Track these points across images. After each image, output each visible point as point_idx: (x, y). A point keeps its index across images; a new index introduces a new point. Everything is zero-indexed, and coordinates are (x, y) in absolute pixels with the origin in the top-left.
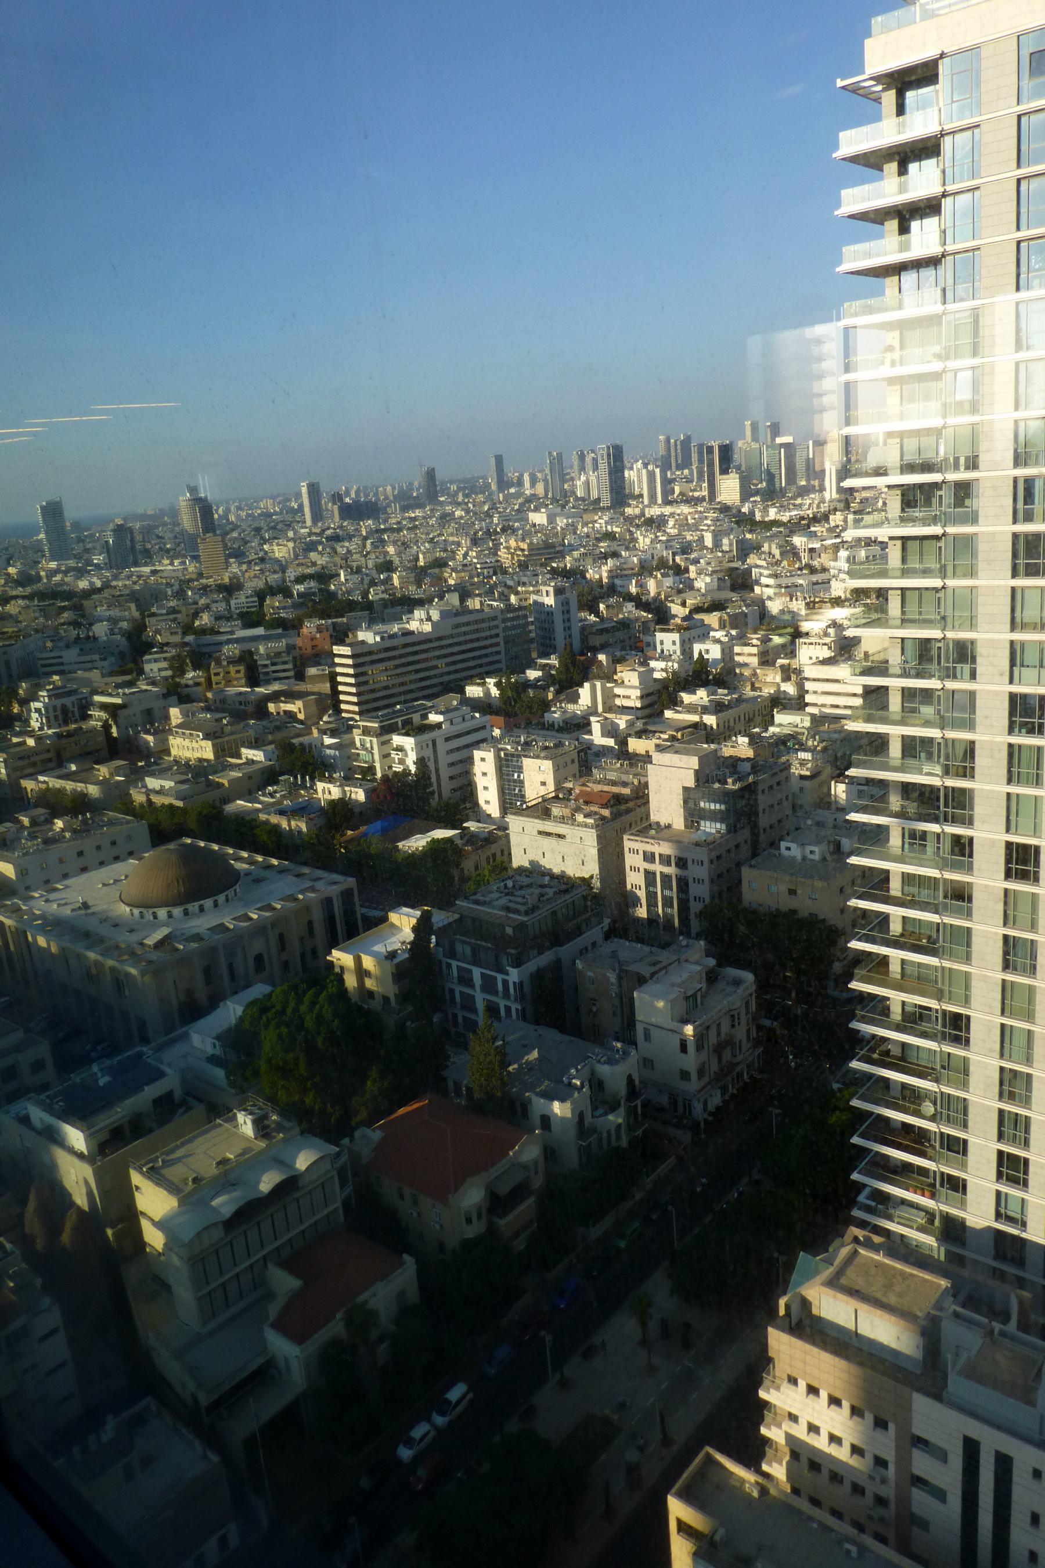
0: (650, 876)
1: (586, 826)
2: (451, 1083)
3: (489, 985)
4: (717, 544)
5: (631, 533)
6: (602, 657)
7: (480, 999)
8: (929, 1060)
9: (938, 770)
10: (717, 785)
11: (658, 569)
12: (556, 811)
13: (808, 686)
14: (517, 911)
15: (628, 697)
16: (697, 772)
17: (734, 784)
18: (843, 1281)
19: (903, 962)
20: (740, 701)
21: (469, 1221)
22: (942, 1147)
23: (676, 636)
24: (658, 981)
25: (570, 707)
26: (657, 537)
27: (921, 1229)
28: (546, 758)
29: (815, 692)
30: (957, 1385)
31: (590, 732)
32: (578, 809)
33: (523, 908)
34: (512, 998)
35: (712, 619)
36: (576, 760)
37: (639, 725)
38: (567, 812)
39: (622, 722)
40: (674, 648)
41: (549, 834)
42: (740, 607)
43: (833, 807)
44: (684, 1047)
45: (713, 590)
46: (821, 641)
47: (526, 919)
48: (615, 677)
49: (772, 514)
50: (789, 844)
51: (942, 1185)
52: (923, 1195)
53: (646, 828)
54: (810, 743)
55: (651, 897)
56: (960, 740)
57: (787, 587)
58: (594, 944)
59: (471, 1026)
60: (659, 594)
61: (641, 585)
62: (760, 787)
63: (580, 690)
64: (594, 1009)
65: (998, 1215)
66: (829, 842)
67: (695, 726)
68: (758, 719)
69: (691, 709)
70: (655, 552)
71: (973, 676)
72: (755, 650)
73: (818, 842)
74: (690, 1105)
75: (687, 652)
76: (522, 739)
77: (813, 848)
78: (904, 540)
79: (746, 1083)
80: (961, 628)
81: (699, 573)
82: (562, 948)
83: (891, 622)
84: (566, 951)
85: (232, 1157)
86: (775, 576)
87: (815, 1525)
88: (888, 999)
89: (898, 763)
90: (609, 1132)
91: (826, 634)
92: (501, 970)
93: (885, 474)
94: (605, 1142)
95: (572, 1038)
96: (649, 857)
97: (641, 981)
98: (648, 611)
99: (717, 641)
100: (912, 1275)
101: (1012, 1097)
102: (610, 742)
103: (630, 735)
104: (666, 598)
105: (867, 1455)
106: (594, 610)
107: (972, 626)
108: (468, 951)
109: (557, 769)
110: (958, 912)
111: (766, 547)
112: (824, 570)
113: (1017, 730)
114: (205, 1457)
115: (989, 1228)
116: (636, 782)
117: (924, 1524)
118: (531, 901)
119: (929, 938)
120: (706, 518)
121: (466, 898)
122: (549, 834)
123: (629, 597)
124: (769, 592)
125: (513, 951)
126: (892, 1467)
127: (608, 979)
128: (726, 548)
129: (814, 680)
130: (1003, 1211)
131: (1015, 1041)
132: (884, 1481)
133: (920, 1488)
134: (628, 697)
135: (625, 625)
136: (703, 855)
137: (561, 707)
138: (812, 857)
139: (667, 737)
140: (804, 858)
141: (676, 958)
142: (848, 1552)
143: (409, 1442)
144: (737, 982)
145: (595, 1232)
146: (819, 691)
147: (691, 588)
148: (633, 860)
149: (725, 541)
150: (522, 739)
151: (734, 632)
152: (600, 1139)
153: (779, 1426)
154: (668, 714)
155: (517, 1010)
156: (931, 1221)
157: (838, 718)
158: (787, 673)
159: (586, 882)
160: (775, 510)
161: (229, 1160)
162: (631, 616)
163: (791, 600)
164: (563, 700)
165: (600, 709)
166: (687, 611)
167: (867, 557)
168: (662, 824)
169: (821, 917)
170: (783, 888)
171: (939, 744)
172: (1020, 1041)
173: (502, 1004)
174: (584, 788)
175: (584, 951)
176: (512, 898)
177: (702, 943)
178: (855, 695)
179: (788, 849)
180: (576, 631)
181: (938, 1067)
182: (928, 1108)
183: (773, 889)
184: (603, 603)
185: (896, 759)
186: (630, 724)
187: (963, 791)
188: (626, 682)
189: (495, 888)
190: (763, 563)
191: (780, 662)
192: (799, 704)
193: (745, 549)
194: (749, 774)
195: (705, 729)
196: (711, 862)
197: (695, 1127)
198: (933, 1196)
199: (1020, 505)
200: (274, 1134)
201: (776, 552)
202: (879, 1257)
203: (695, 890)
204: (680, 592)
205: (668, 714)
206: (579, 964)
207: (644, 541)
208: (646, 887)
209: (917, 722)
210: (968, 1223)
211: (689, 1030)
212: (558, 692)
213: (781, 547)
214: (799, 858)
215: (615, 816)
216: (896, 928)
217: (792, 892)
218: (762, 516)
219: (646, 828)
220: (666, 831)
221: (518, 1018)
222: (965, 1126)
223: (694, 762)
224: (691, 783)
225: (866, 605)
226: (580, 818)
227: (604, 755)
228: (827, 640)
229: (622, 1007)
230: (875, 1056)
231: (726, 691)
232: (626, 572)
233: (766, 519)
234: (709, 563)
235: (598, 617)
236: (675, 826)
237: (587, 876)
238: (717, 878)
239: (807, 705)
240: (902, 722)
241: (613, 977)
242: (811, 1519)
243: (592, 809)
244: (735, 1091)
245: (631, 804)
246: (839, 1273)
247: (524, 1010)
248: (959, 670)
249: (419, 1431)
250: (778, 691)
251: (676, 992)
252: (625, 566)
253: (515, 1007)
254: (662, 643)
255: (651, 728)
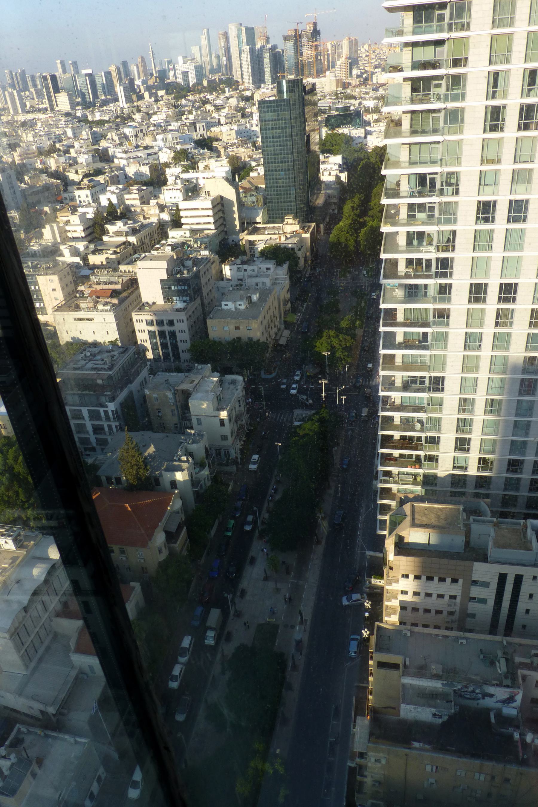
0: (152, 334)
1: (106, 311)
2: (104, 479)
3: (95, 415)
4: (76, 136)
5: (17, 132)
6: (46, 209)
7: (89, 425)
8: (415, 403)
9: (432, 249)
10: (178, 276)
11: (54, 152)
12: (83, 305)
13: (182, 213)
14: (102, 369)
15: (75, 231)
16: (167, 270)
17: (188, 273)
18: (417, 522)
19: (403, 356)
20: (143, 226)
21: (160, 551)
22: (426, 443)
23: (88, 192)
24: (197, 391)
25: (41, 241)
26: (35, 133)
27: (413, 484)
28: (53, 274)
29: (186, 217)
30: (492, 552)
31: (62, 255)
32: (97, 302)
33: (106, 367)
34: (112, 420)
35: (101, 179)
36: (70, 273)
37: (92, 246)
38: (91, 305)
39: (81, 246)
40: (87, 199)
41: (81, 320)
42: (113, 172)
43: (225, 279)
44: (222, 423)
45: (90, 163)
46: (175, 188)
47: (110, 373)
48: (58, 220)
49: (98, 116)
50: (226, 303)
51: (425, 461)
52: (415, 468)
53: (141, 307)
54: (196, 246)
55: (154, 347)
56: (446, 231)
57: (134, 158)
58: (145, 379)
59: (85, 441)
60: (58, 167)
61: (42, 162)
62: (202, 273)
63: (43, 230)
64: (160, 414)
65: (454, 467)
66: (247, 298)
67: (124, 243)
68: (156, 236)
69: (118, 234)
70: (42, 142)
71: (457, 192)
72: (137, 196)
73: (241, 299)
74: (228, 452)
75: (96, 200)
76: (30, 265)
77: (240, 303)
78: (412, 112)
79: (247, 433)
80: (451, 165)
81: (78, 152)
82: (133, 384)
83: (403, 165)
84: (134, 386)
85: (7, 566)
86: (125, 152)
87: (440, 638)
88: (394, 376)
89: (404, 248)
90: (204, 479)
91: (176, 183)
92: (102, 405)
93: (401, 70)
94: (203, 485)
95: (167, 434)
96: (150, 323)
97: (187, 395)
98: (57, 179)
99: (113, 193)
100: (443, 508)
101: (464, 411)
102: (77, 260)
103: (89, 254)
104: (64, 170)
105: (421, 594)
106: (22, 181)
107: (459, 164)
108: (77, 398)
109: (60, 279)
110: (440, 324)
111: (109, 136)
112: (152, 147)
113: (479, 222)
114: (76, 742)
115: (449, 475)
116: (120, 280)
117: (473, 616)
118: (108, 360)
119: (419, 341)
120: (60, 120)
121: (65, 367)
122: (81, 320)
123: (42, 171)
124: (123, 163)
125: (109, 393)
126: (458, 599)
127: (166, 397)
128: (86, 138)
129: (185, 210)
130: (455, 465)
131: (467, 385)
132: (455, 604)
133: (472, 602)
134: (75, 231)
135: (47, 188)
136: (183, 316)
137: (36, 242)
138: (241, 307)
139: (112, 252)
140: (236, 308)
141: (201, 376)
142: (462, 643)
143: (174, 678)
144: (234, 382)
145: (213, 532)
146: (189, 215)
147: (77, 163)
148: (138, 326)
149: (84, 133)
150: (30, 265)
151: (121, 187)
152: (201, 485)
153: (396, 598)
154: (105, 238)
155: (116, 426)
156: (415, 479)
157: (202, 230)
158: (162, 208)
159: (112, 343)
160: (99, 113)
161: (6, 568)
162: (48, 182)
163: (140, 165)
164: (32, 238)
165: (59, 241)
166: (81, 177)
167: (173, 138)
168: (150, 302)
169: (255, 339)
170: (232, 327)
171: (429, 235)
172: (470, 383)
173: (105, 425)
174: (91, 289)
175: (144, 384)
176: (94, 362)
177: (209, 365)
178: (209, 216)
179: (226, 305)
180: (18, 194)
181: (426, 405)
182: (418, 426)
183: (226, 328)
184: (27, 175)
185: (402, 246)
186: (87, 247)
187: (447, 259)
188: (72, 222)
189: (80, 358)
190: (111, 145)
191: (153, 202)
192: (177, 223)
193: (96, 138)
194: (193, 267)
195: (130, 245)
196: (188, 320)
197: (235, 462)
198: (420, 467)
199: (491, 90)
200: (25, 543)
201: (116, 138)
202: (426, 505)
203: (180, 336)
204: (71, 165)
205: (105, 238)
206: (147, 392)
207: (28, 137)
208: (150, 341)
209: (416, 223)
210: (438, 476)
211: (224, 414)
212: (26, 232)
213: (118, 135)
214: (234, 309)
215: (121, 302)
216: (400, 339)
217: (237, 328)
218: (92, 118)
219: (141, 307)
220: (154, 306)
221: (117, 431)
222: (439, 430)
223: (164, 264)
224: (165, 277)
225: (183, 166)
226: (100, 307)
227: (95, 268)
228: (179, 187)
229: (178, 409)
230: (388, 407)
231: (131, 222)
232: (30, 156)
233: (95, 120)
234: (81, 147)
235: (25, 184)
236: (158, 303)
237: (113, 339)
238: (191, 328)
239: (183, 224)
240: (408, 224)
241: (170, 394)
242: (437, 635)
243: (106, 300)
244: (245, 439)
245: (125, 294)
246: (413, 519)
247: (120, 425)
248: (445, 191)
249: (177, 670)
250: (159, 219)
251: (212, 396)
252: (29, 152)
253: (114, 424)
254: (79, 196)
255: (99, 248)
